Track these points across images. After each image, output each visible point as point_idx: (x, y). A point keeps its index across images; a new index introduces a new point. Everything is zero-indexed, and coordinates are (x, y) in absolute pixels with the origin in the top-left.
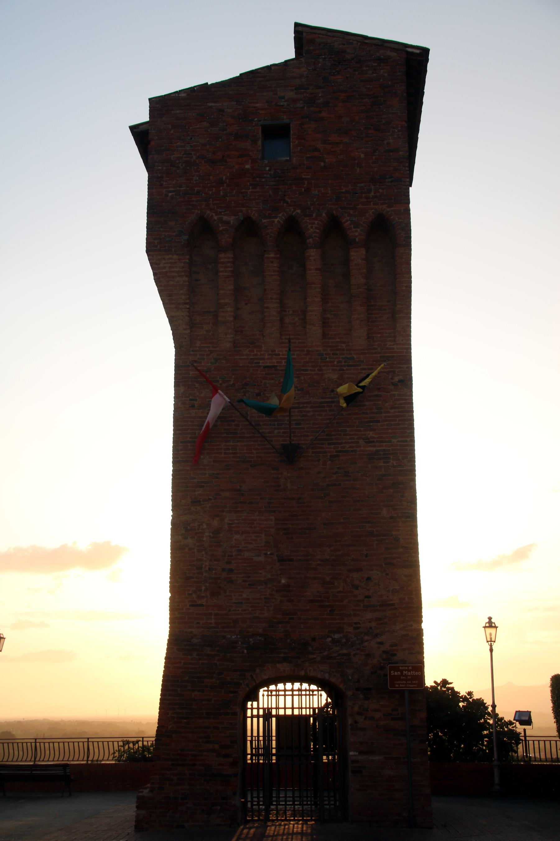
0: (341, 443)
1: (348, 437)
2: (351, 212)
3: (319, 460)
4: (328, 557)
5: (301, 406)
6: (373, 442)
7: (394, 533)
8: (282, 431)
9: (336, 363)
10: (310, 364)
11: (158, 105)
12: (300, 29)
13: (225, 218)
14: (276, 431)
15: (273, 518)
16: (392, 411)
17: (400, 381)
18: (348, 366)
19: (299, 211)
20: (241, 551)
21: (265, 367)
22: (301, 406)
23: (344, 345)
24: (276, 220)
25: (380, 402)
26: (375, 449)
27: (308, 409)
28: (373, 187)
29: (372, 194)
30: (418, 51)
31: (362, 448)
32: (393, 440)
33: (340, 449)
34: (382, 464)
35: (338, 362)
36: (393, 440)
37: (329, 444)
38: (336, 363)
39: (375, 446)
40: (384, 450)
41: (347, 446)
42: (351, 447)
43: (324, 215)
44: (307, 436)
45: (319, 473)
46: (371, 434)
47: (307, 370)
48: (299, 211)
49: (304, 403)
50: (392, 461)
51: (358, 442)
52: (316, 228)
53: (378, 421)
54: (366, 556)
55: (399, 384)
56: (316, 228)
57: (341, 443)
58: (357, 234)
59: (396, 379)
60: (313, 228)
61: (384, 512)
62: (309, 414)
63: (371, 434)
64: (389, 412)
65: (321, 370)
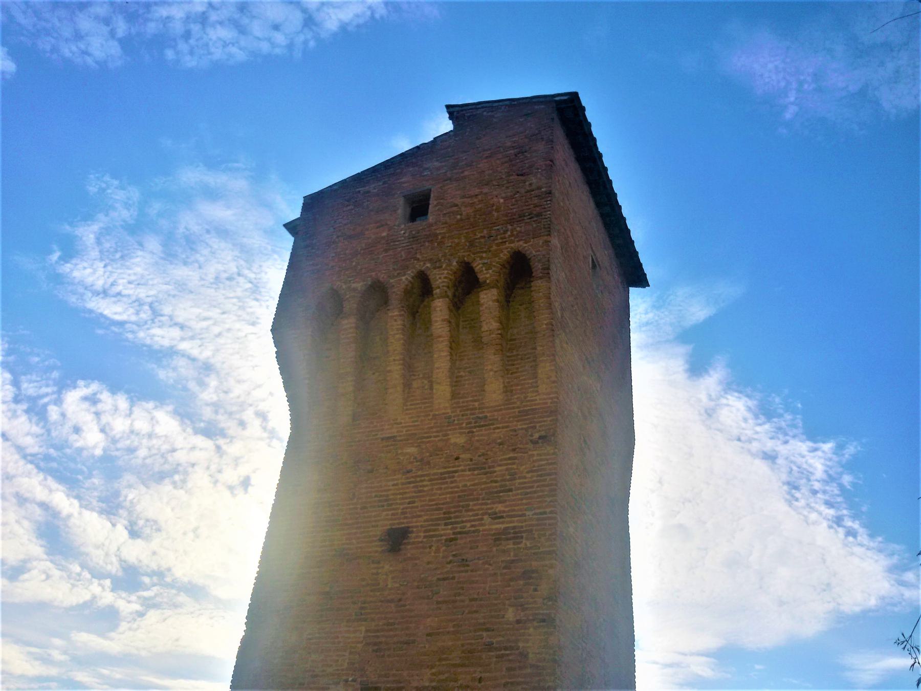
0: (463, 522)
1: (471, 514)
2: (484, 255)
3: (430, 547)
4: (427, 684)
5: (418, 479)
6: (502, 517)
7: (521, 645)
8: (390, 513)
9: (464, 425)
10: (434, 430)
11: (312, 203)
12: (452, 110)
13: (354, 285)
14: (385, 513)
15: (363, 629)
16: (529, 475)
17: (540, 438)
18: (479, 427)
19: (428, 265)
20: (316, 676)
21: (382, 439)
22: (418, 479)
23: (476, 404)
24: (403, 278)
25: (515, 466)
26: (502, 526)
27: (425, 483)
28: (510, 227)
29: (509, 233)
30: (565, 98)
31: (487, 527)
32: (527, 513)
33: (459, 530)
34: (512, 546)
35: (467, 424)
36: (527, 513)
37: (446, 524)
38: (464, 425)
39: (502, 523)
40: (514, 528)
41: (468, 525)
42: (472, 526)
43: (455, 263)
44: (420, 516)
45: (429, 563)
46: (500, 507)
47: (430, 437)
48: (428, 265)
49: (422, 476)
50: (524, 541)
51: (482, 519)
52: (445, 278)
53: (510, 490)
54: (480, 680)
55: (540, 441)
56: (445, 278)
57: (463, 522)
58: (488, 276)
59: (536, 435)
60: (441, 279)
61: (511, 615)
62: (425, 489)
63: (500, 507)
64: (525, 478)
65: (448, 435)
